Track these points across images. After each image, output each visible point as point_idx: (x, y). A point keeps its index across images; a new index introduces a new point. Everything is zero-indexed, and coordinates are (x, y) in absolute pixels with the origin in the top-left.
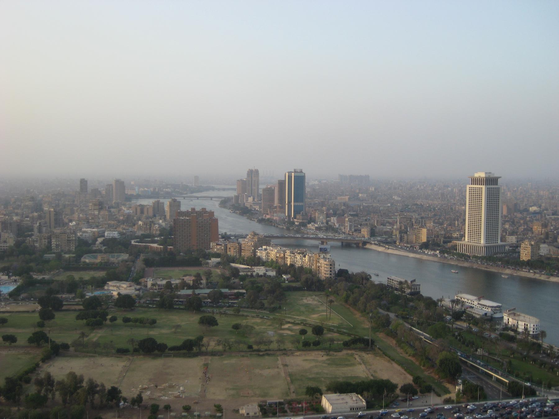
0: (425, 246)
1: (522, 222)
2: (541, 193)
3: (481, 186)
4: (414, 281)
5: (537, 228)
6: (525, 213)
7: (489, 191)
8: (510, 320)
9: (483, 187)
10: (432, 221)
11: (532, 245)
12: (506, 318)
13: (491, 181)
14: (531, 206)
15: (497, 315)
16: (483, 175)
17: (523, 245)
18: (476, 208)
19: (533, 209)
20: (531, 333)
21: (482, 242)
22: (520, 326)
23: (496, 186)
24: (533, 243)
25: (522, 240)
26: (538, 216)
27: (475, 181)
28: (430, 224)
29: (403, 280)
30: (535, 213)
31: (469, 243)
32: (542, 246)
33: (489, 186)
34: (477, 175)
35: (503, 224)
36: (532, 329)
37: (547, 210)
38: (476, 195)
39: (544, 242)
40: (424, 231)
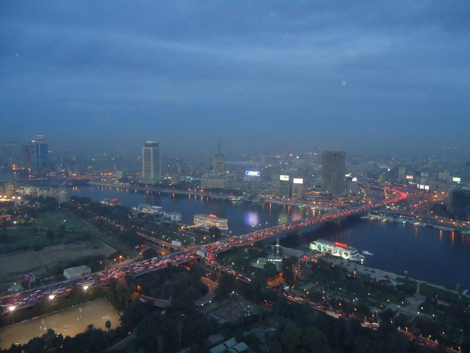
7: (154, 150)
12: (165, 214)
15: (160, 213)
16: (150, 142)
21: (152, 176)
27: (147, 145)
32: (182, 177)
34: (147, 142)
38: (147, 152)
39: (182, 175)
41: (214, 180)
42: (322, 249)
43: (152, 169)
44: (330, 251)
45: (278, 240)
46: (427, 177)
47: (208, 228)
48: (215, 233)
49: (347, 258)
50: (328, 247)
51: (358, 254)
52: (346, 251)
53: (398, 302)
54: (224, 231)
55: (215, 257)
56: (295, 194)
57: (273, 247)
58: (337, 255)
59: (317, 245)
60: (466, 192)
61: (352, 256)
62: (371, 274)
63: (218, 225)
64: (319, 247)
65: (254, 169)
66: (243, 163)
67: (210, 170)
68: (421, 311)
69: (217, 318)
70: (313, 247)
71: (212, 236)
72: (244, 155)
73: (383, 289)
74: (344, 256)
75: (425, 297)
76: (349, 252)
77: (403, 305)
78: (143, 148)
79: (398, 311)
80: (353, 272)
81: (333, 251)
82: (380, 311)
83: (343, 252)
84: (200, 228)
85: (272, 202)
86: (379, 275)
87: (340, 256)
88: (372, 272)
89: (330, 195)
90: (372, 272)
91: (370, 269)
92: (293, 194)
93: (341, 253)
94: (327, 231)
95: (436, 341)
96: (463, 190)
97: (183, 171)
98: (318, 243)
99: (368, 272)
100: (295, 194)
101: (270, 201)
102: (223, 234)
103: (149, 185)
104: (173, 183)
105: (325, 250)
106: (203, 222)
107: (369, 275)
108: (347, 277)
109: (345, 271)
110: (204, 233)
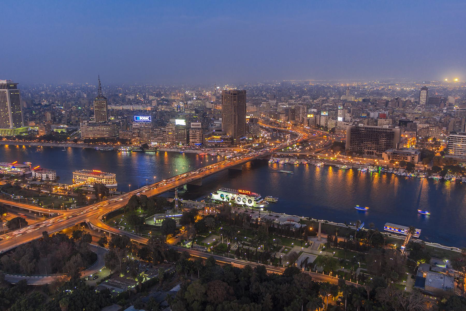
6: (39, 107)
8: (37, 174)
9: (7, 90)
11: (45, 126)
12: (33, 173)
15: (27, 173)
16: (5, 82)
20: (51, 179)
22: (43, 177)
26: (48, 108)
30: (46, 106)
36: (51, 177)
37: (53, 103)
41: (95, 128)
42: (225, 197)
43: (10, 117)
44: (233, 199)
45: (406, 242)
46: (326, 116)
47: (92, 186)
48: (101, 192)
49: (251, 205)
50: (230, 196)
51: (262, 199)
52: (249, 198)
53: (301, 244)
54: (113, 187)
55: (103, 218)
58: (241, 203)
59: (219, 195)
60: (362, 129)
61: (256, 202)
63: (104, 181)
64: (222, 196)
65: (144, 113)
66: (130, 108)
67: (90, 116)
68: (323, 250)
69: (109, 287)
70: (216, 197)
71: (97, 195)
72: (132, 97)
73: (287, 233)
74: (247, 204)
75: (326, 236)
76: (253, 199)
77: (307, 247)
79: (301, 252)
80: (257, 220)
81: (236, 199)
82: (284, 254)
83: (247, 200)
84: (81, 186)
85: (169, 150)
86: (283, 218)
87: (243, 203)
88: (277, 217)
89: (232, 139)
91: (274, 214)
92: (191, 140)
93: (245, 200)
94: (230, 178)
95: (337, 276)
96: (359, 127)
97: (54, 119)
98: (220, 193)
99: (272, 218)
101: (165, 150)
102: (111, 191)
103: (8, 138)
104: (42, 134)
106: (85, 179)
108: (252, 225)
109: (249, 218)
110: (86, 193)
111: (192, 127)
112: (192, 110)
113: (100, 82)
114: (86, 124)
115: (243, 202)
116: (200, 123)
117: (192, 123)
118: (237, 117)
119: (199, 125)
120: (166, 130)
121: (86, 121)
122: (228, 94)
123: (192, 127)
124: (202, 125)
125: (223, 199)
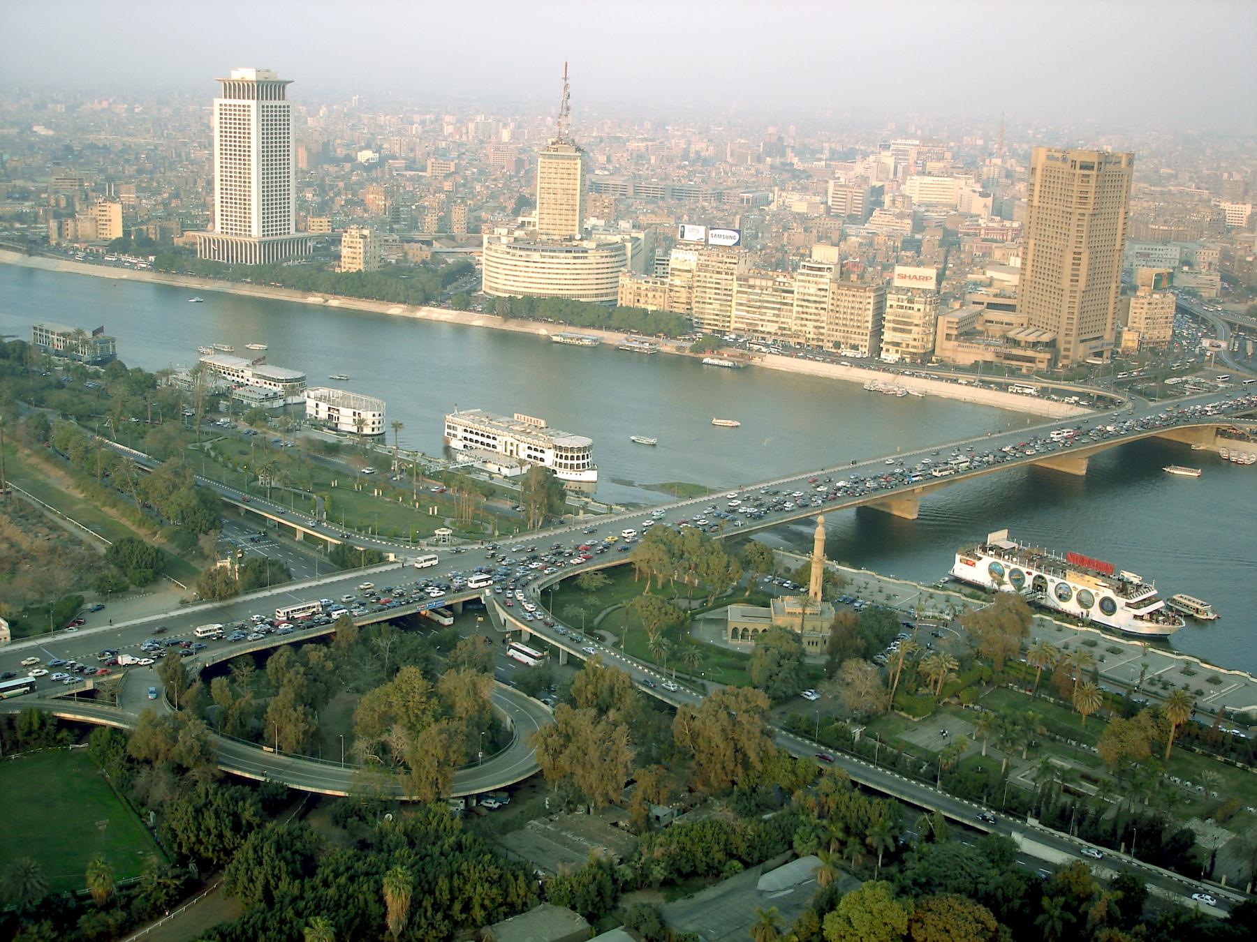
0: (120, 246)
1: (341, 184)
2: (382, 120)
3: (246, 102)
4: (101, 330)
5: (376, 199)
6: (348, 166)
7: (264, 112)
10: (133, 186)
11: (365, 237)
13: (269, 89)
14: (361, 149)
17: (346, 238)
18: (237, 153)
19: (365, 156)
21: (256, 232)
23: (282, 103)
24: (366, 232)
25: (345, 226)
27: (234, 89)
28: (129, 196)
29: (71, 330)
30: (369, 167)
31: (225, 237)
33: (265, 103)
34: (236, 75)
35: (300, 189)
37: (394, 158)
40: (115, 213)
42: (1006, 578)
56: (898, 337)
57: (793, 560)
62: (1205, 686)
63: (549, 459)
64: (994, 571)
67: (516, 212)
78: (217, 102)
81: (1051, 588)
90: (1215, 680)
92: (888, 336)
94: (1033, 499)
99: (1195, 683)
100: (898, 337)
105: (1020, 588)
107: (1199, 693)
111: (897, 282)
112: (901, 216)
113: (566, 87)
114: (504, 240)
115: (1080, 602)
116: (932, 272)
117: (899, 269)
118: (1085, 257)
119: (926, 278)
120: (795, 286)
121: (505, 231)
122: (1059, 164)
123: (897, 282)
124: (939, 282)
125: (1000, 583)
